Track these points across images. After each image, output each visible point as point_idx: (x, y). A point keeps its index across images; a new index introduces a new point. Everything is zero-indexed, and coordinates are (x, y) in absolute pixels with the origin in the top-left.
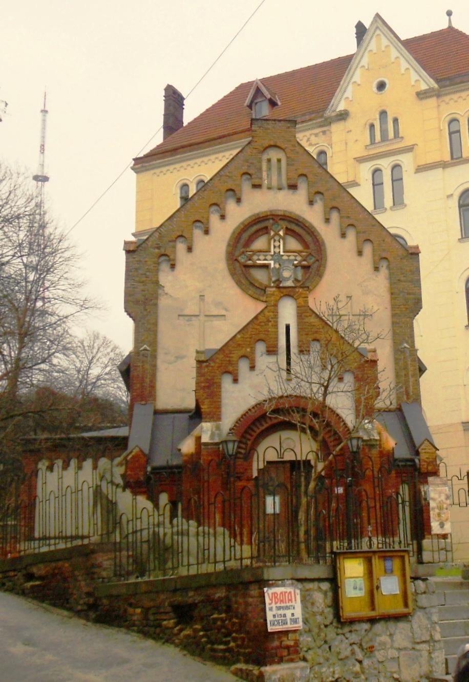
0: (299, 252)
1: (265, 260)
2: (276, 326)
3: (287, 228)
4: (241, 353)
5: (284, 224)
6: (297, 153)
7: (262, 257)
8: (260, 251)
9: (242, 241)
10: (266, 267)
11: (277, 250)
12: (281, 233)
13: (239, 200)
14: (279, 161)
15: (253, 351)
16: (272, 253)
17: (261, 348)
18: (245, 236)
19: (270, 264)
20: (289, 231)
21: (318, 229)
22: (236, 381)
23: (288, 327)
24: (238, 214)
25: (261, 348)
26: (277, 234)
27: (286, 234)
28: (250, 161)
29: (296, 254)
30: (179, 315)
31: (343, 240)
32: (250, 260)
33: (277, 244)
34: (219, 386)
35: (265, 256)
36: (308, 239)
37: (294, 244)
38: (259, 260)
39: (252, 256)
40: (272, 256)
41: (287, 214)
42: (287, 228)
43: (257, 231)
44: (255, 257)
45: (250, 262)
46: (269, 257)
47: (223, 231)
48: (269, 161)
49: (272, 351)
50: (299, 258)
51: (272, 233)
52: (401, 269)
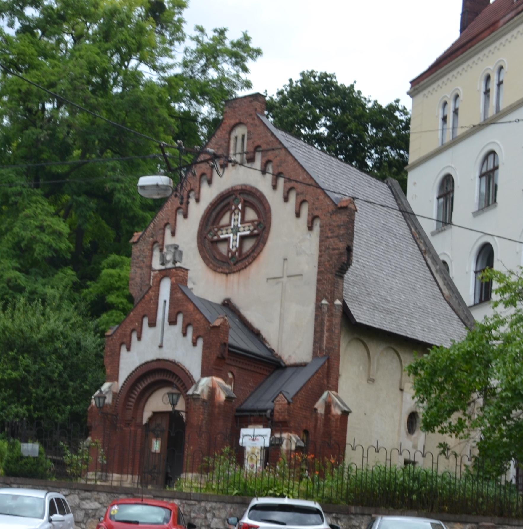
0: (252, 222)
1: (227, 233)
2: (157, 304)
3: (245, 201)
4: (132, 327)
5: (241, 197)
6: (256, 125)
7: (224, 232)
8: (223, 226)
9: (212, 219)
10: (227, 240)
11: (236, 223)
12: (240, 207)
13: (210, 182)
14: (243, 136)
15: (141, 324)
16: (232, 226)
17: (146, 321)
18: (214, 214)
19: (229, 238)
20: (246, 203)
21: (267, 198)
22: (128, 349)
23: (165, 301)
24: (209, 194)
25: (146, 321)
26: (237, 208)
27: (244, 207)
28: (219, 143)
29: (250, 224)
30: (268, 279)
31: (286, 204)
32: (215, 235)
33: (236, 217)
34: (119, 354)
35: (227, 230)
36: (260, 207)
37: (251, 215)
38: (222, 234)
39: (217, 232)
40: (232, 229)
41: (244, 187)
42: (245, 201)
43: (224, 207)
44: (220, 233)
45: (215, 238)
46: (230, 231)
47: (197, 211)
48: (236, 138)
49: (152, 324)
50: (252, 228)
51: (233, 207)
52: (330, 225)
